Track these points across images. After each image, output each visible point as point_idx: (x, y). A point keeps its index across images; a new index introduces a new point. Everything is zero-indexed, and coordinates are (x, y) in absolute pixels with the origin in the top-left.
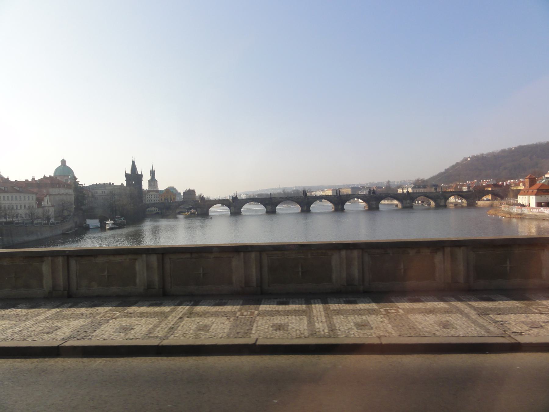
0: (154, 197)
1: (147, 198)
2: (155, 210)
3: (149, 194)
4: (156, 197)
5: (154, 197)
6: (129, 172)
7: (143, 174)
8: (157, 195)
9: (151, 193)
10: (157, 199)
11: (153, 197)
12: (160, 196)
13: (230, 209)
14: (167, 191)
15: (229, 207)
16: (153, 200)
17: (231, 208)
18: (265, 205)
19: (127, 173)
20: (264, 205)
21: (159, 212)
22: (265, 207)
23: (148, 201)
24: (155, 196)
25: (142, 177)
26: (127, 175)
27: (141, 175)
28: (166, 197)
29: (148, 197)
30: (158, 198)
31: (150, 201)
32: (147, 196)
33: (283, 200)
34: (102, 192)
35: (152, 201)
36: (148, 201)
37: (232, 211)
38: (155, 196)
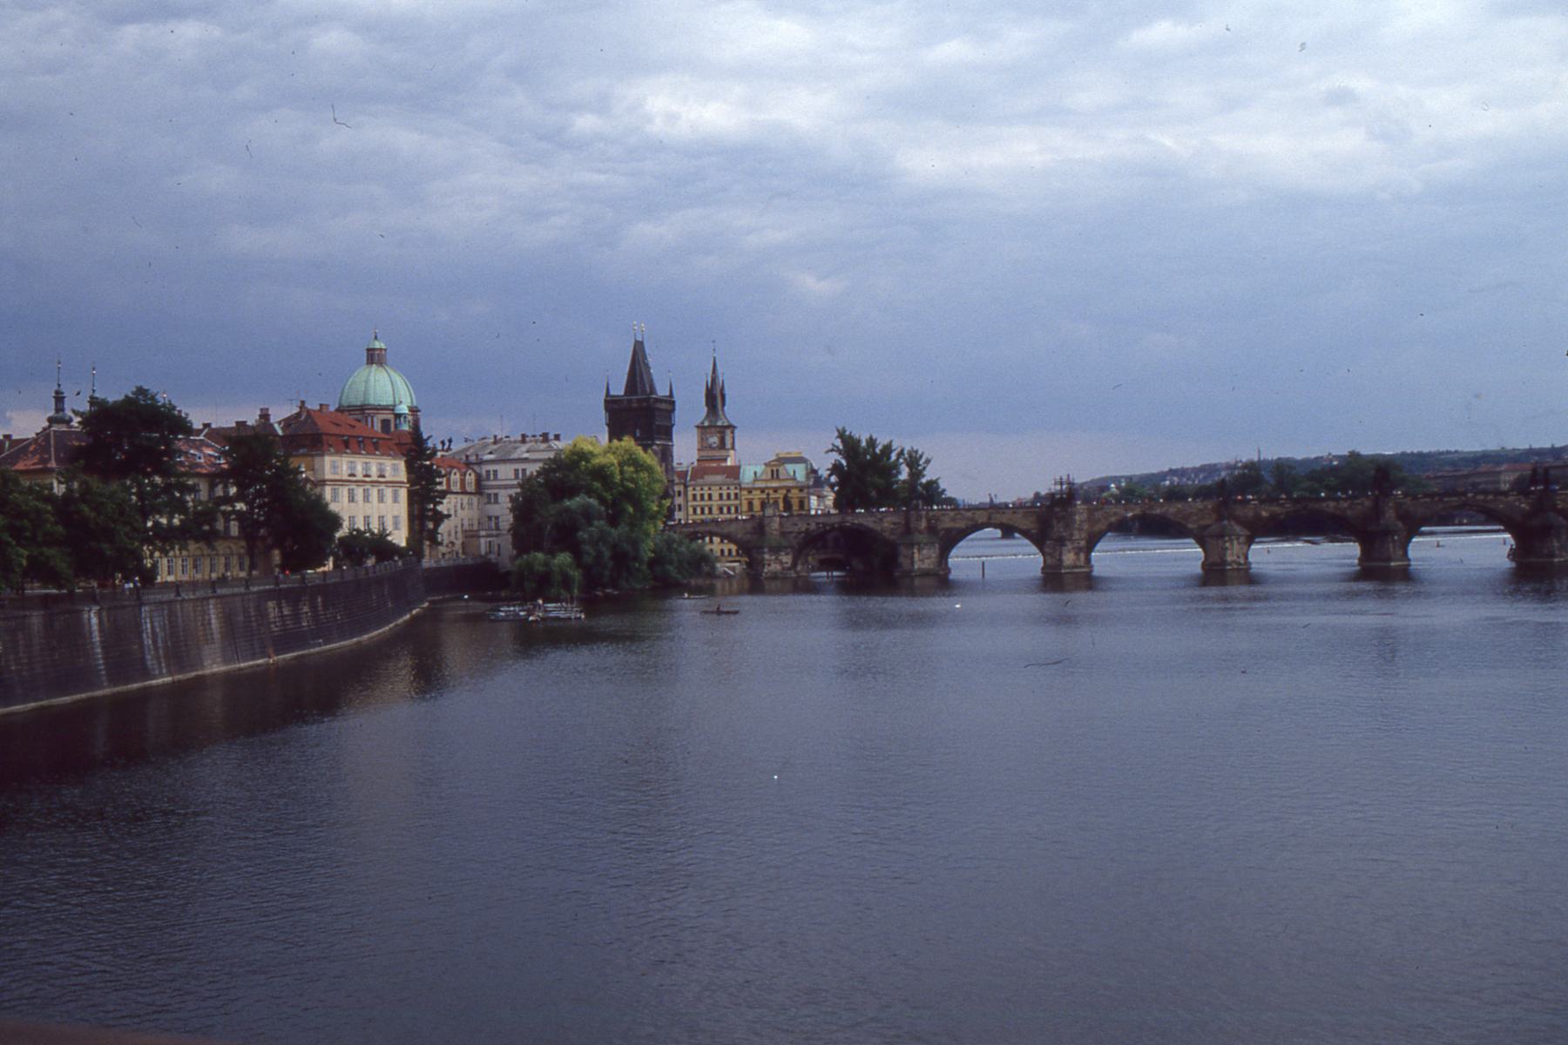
0: (721, 495)
1: (690, 497)
2: (722, 551)
3: (700, 481)
4: (729, 496)
5: (721, 495)
6: (619, 390)
7: (676, 398)
8: (732, 487)
11: (715, 496)
12: (745, 492)
14: (772, 471)
16: (715, 510)
19: (612, 393)
25: (674, 410)
26: (612, 405)
27: (670, 402)
28: (768, 494)
29: (694, 496)
30: (736, 494)
32: (690, 492)
34: (516, 471)
35: (710, 512)
37: (1049, 561)
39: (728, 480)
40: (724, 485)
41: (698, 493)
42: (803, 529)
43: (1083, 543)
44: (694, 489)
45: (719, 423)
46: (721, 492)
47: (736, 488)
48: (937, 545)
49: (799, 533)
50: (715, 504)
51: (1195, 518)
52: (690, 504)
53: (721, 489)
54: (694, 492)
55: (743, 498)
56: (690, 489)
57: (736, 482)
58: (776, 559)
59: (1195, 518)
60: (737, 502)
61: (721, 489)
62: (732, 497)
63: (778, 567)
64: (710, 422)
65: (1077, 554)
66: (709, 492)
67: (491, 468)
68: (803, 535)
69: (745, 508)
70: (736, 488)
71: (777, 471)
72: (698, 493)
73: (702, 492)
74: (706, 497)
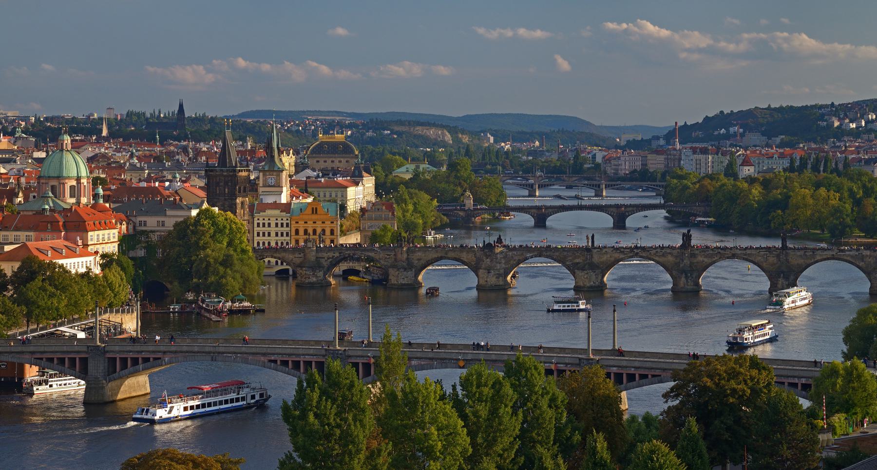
1: (256, 225)
5: (277, 225)
8: (285, 219)
9: (269, 212)
10: (285, 229)
11: (273, 225)
12: (294, 222)
13: (477, 275)
14: (313, 209)
15: (475, 269)
17: (481, 271)
18: (573, 269)
20: (568, 268)
21: (288, 267)
22: (574, 274)
23: (258, 235)
24: (279, 222)
29: (258, 225)
30: (287, 226)
31: (264, 235)
33: (622, 256)
36: (258, 235)
38: (279, 222)
39: (282, 213)
40: (279, 217)
41: (261, 222)
42: (331, 256)
43: (502, 271)
44: (258, 219)
45: (276, 169)
46: (277, 222)
47: (287, 220)
48: (414, 270)
49: (328, 258)
50: (273, 230)
51: (570, 258)
52: (255, 229)
53: (277, 219)
54: (258, 221)
55: (292, 226)
56: (256, 219)
57: (289, 215)
58: (313, 274)
59: (570, 258)
60: (288, 229)
61: (277, 219)
62: (285, 225)
63: (314, 279)
64: (269, 167)
65: (497, 278)
66: (269, 221)
67: (142, 219)
68: (331, 260)
69: (293, 233)
70: (287, 220)
71: (316, 209)
72: (261, 222)
73: (264, 221)
74: (266, 225)
